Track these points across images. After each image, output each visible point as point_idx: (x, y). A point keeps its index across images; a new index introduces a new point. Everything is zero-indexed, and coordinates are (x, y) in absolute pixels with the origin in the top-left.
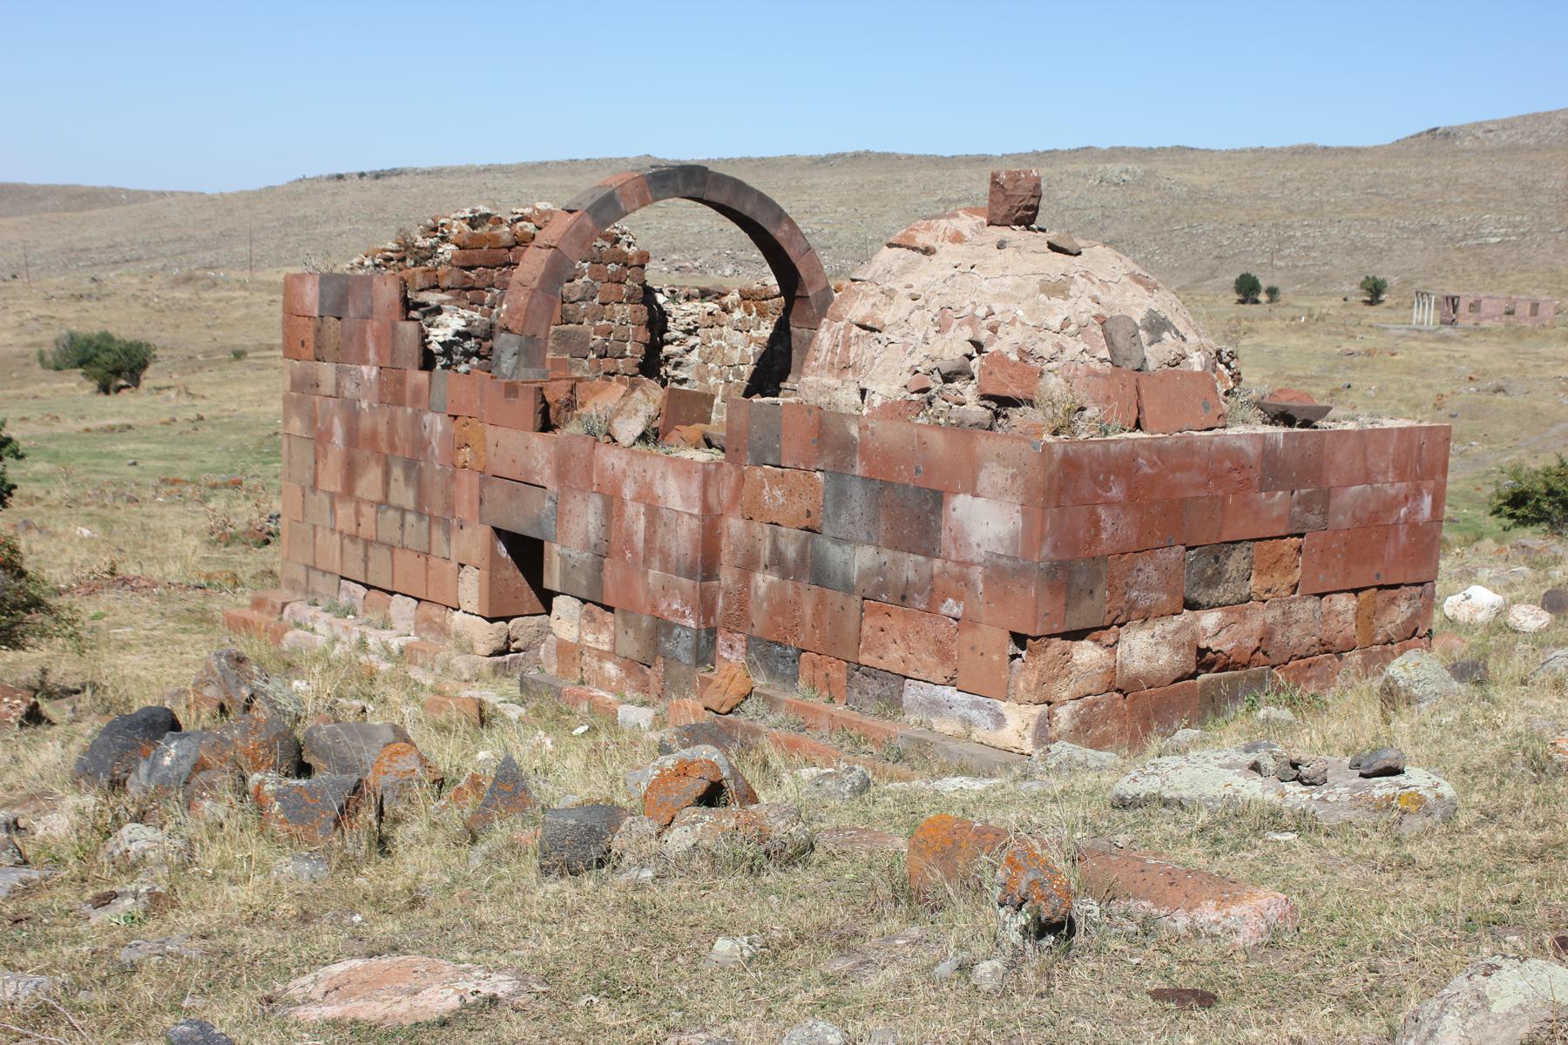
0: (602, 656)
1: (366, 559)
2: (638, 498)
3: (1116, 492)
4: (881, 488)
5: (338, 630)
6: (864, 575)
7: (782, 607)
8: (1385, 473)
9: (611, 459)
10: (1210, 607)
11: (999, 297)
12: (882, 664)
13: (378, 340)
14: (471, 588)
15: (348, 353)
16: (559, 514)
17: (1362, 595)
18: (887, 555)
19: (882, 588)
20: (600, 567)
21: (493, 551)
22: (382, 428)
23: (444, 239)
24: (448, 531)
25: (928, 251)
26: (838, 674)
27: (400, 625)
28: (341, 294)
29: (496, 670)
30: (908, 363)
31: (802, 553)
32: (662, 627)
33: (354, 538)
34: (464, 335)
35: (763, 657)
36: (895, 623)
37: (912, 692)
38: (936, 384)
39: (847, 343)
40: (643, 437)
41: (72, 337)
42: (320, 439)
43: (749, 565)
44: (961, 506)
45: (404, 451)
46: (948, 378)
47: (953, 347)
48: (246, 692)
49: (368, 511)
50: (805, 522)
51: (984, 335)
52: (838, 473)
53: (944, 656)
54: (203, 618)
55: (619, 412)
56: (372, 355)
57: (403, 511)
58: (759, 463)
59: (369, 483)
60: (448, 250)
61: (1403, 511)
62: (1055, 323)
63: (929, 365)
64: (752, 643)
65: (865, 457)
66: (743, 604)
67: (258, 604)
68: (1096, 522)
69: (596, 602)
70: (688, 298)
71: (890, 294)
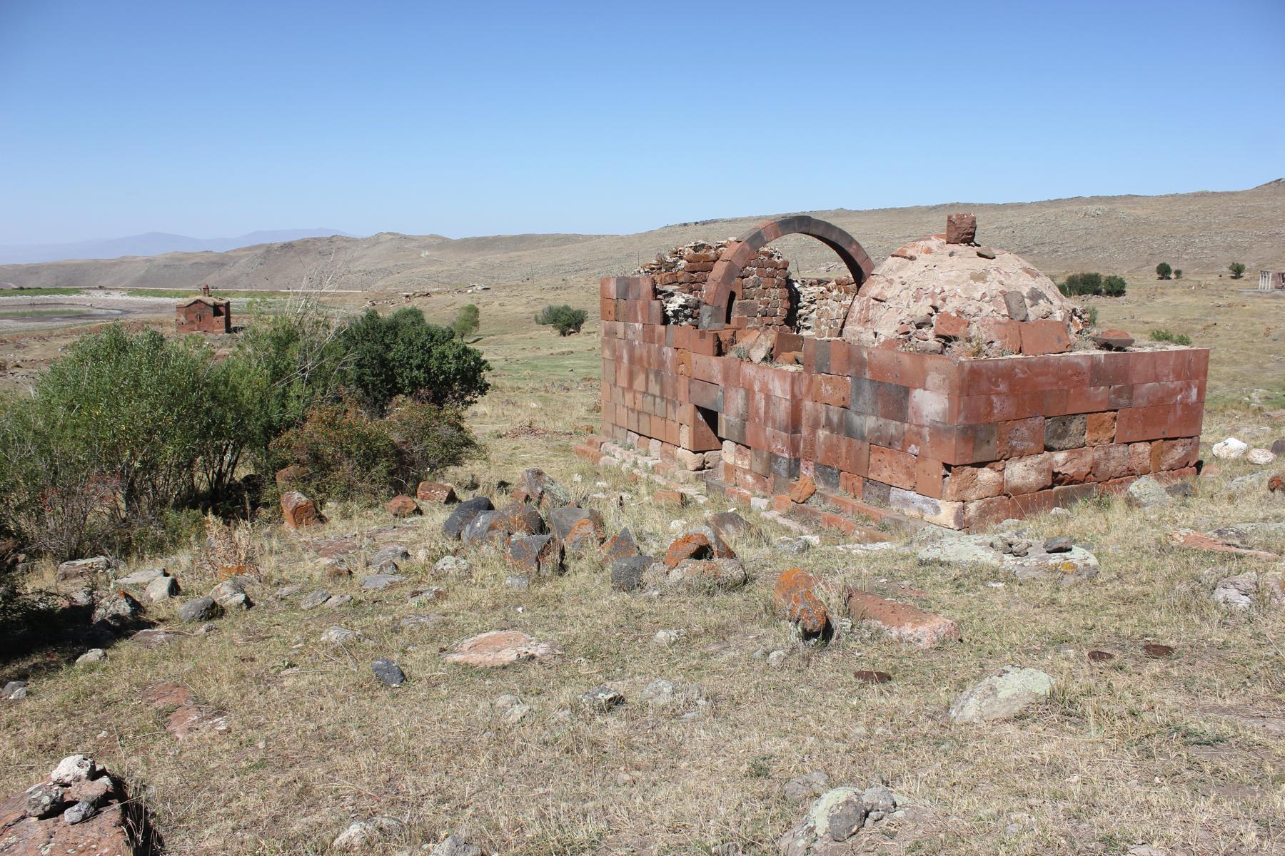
0: (745, 472)
1: (638, 421)
2: (761, 391)
3: (1003, 387)
4: (878, 385)
5: (625, 457)
6: (871, 431)
7: (832, 448)
8: (1168, 376)
9: (748, 370)
10: (1060, 450)
11: (948, 282)
12: (879, 479)
13: (642, 309)
14: (685, 436)
15: (629, 317)
16: (725, 398)
18: (882, 421)
19: (879, 438)
20: (744, 426)
21: (696, 420)
22: (645, 355)
23: (681, 258)
24: (675, 407)
25: (912, 258)
26: (858, 484)
27: (654, 454)
28: (626, 286)
29: (697, 478)
30: (899, 318)
31: (841, 419)
32: (773, 458)
33: (633, 410)
34: (684, 307)
35: (822, 474)
36: (886, 457)
37: (895, 494)
38: (912, 329)
39: (868, 309)
40: (765, 359)
41: (550, 308)
42: (617, 359)
43: (815, 426)
44: (918, 395)
45: (655, 366)
46: (919, 326)
47: (922, 309)
48: (540, 490)
49: (639, 396)
50: (842, 403)
51: (938, 303)
52: (858, 377)
53: (910, 475)
54: (566, 450)
55: (752, 346)
56: (640, 318)
57: (655, 396)
58: (820, 372)
59: (639, 383)
60: (683, 263)
62: (978, 295)
63: (909, 319)
64: (818, 466)
65: (871, 369)
66: (812, 446)
67: (590, 443)
68: (990, 404)
69: (742, 444)
70: (811, 285)
71: (891, 282)
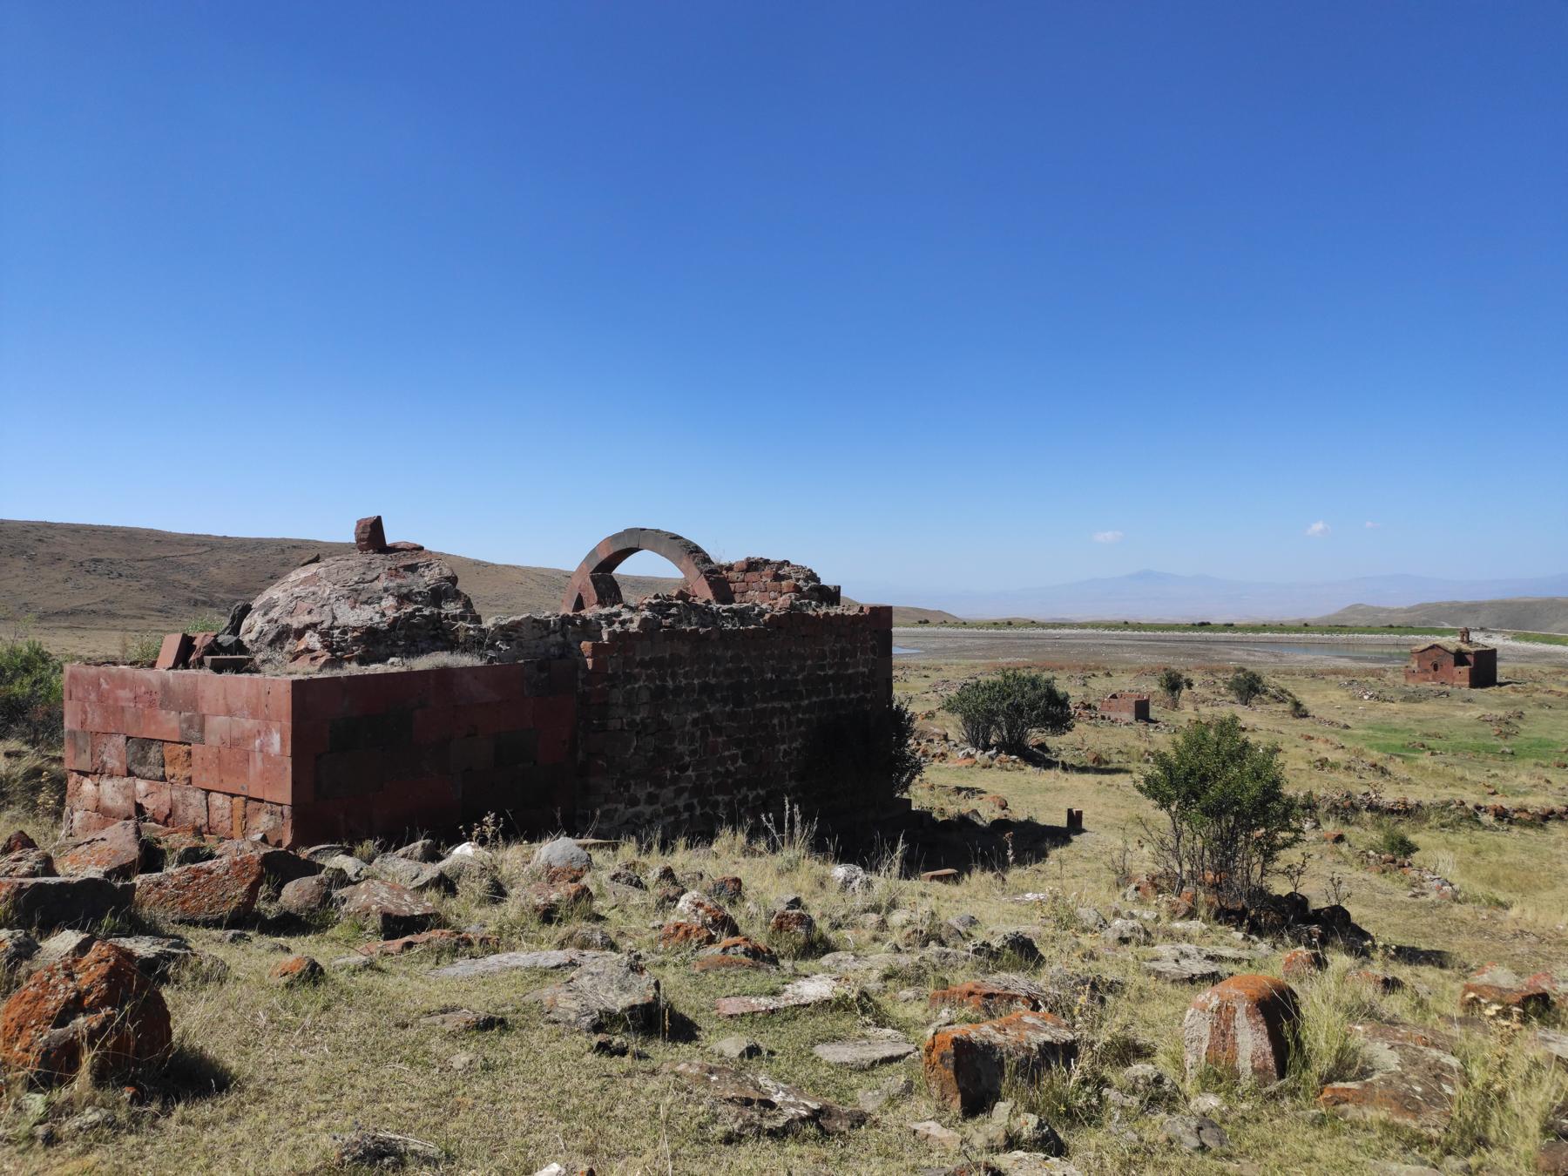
3: (93, 697)
61: (258, 742)
68: (85, 712)
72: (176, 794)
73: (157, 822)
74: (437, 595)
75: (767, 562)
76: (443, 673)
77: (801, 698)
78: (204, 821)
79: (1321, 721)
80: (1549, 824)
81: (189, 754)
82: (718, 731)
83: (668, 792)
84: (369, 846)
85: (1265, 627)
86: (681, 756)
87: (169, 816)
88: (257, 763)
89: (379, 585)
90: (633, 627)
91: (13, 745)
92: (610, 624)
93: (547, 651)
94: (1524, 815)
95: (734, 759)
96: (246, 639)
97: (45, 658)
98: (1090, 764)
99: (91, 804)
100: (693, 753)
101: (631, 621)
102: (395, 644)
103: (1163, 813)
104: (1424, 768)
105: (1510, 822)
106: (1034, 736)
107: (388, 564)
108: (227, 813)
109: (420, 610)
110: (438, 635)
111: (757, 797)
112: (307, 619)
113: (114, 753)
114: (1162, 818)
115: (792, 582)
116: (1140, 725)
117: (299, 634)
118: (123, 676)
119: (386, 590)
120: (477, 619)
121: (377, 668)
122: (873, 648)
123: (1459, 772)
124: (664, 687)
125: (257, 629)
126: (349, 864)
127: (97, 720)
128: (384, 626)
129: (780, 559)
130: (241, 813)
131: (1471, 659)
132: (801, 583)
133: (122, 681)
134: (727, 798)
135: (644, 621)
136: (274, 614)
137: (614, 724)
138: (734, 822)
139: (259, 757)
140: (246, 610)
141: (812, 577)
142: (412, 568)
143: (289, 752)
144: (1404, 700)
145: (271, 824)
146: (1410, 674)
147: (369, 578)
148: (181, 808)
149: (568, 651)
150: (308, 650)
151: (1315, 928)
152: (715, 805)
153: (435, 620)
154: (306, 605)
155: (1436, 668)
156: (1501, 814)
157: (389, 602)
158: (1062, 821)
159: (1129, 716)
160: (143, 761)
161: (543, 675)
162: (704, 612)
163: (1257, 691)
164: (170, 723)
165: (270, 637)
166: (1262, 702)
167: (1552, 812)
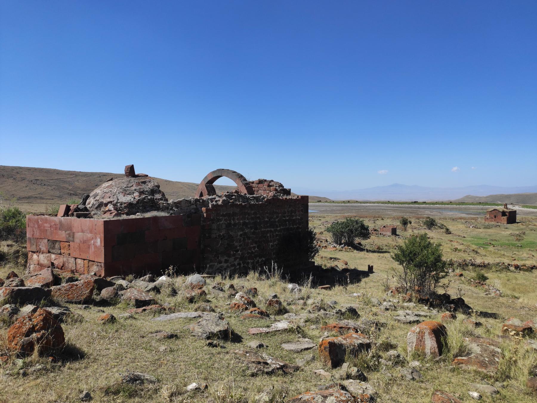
3: (36, 226)
17: (85, 261)
61: (92, 242)
68: (34, 231)
72: (65, 259)
73: (58, 268)
74: (153, 192)
75: (265, 181)
76: (155, 218)
77: (277, 227)
78: (75, 268)
79: (455, 235)
80: (533, 270)
81: (69, 245)
82: (249, 238)
83: (232, 259)
84: (131, 277)
85: (436, 203)
86: (236, 247)
87: (63, 266)
88: (92, 249)
89: (133, 188)
90: (220, 203)
91: (10, 242)
92: (212, 202)
93: (191, 211)
94: (525, 267)
95: (254, 248)
96: (88, 207)
97: (20, 213)
98: (376, 250)
99: (36, 262)
100: (240, 246)
101: (219, 201)
102: (138, 208)
103: (401, 266)
104: (491, 251)
105: (520, 270)
106: (357, 240)
107: (136, 181)
108: (82, 266)
109: (147, 197)
110: (153, 205)
111: (262, 261)
112: (109, 200)
113: (43, 245)
114: (400, 268)
115: (274, 187)
116: (393, 236)
117: (106, 205)
118: (46, 220)
119: (135, 190)
120: (167, 200)
121: (132, 217)
122: (302, 210)
123: (502, 252)
124: (230, 223)
125: (92, 203)
126: (124, 283)
127: (38, 234)
128: (135, 202)
129: (270, 180)
130: (87, 265)
131: (507, 214)
132: (277, 188)
133: (46, 221)
134: (252, 261)
135: (224, 201)
136: (97, 198)
137: (214, 236)
138: (254, 269)
139: (93, 247)
140: (88, 197)
141: (281, 186)
142: (144, 183)
143: (103, 245)
144: (484, 228)
145: (97, 269)
146: (486, 219)
147: (129, 186)
148: (66, 264)
149: (197, 211)
150: (109, 210)
151: (452, 305)
152: (248, 263)
153: (152, 200)
154: (108, 195)
155: (495, 217)
156: (517, 267)
157: (136, 194)
158: (366, 269)
159: (389, 233)
160: (54, 248)
161: (189, 219)
162: (244, 198)
163: (434, 225)
164: (62, 235)
165: (96, 206)
166: (435, 228)
167: (534, 266)
